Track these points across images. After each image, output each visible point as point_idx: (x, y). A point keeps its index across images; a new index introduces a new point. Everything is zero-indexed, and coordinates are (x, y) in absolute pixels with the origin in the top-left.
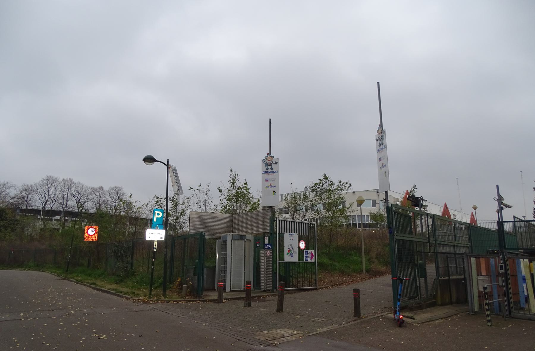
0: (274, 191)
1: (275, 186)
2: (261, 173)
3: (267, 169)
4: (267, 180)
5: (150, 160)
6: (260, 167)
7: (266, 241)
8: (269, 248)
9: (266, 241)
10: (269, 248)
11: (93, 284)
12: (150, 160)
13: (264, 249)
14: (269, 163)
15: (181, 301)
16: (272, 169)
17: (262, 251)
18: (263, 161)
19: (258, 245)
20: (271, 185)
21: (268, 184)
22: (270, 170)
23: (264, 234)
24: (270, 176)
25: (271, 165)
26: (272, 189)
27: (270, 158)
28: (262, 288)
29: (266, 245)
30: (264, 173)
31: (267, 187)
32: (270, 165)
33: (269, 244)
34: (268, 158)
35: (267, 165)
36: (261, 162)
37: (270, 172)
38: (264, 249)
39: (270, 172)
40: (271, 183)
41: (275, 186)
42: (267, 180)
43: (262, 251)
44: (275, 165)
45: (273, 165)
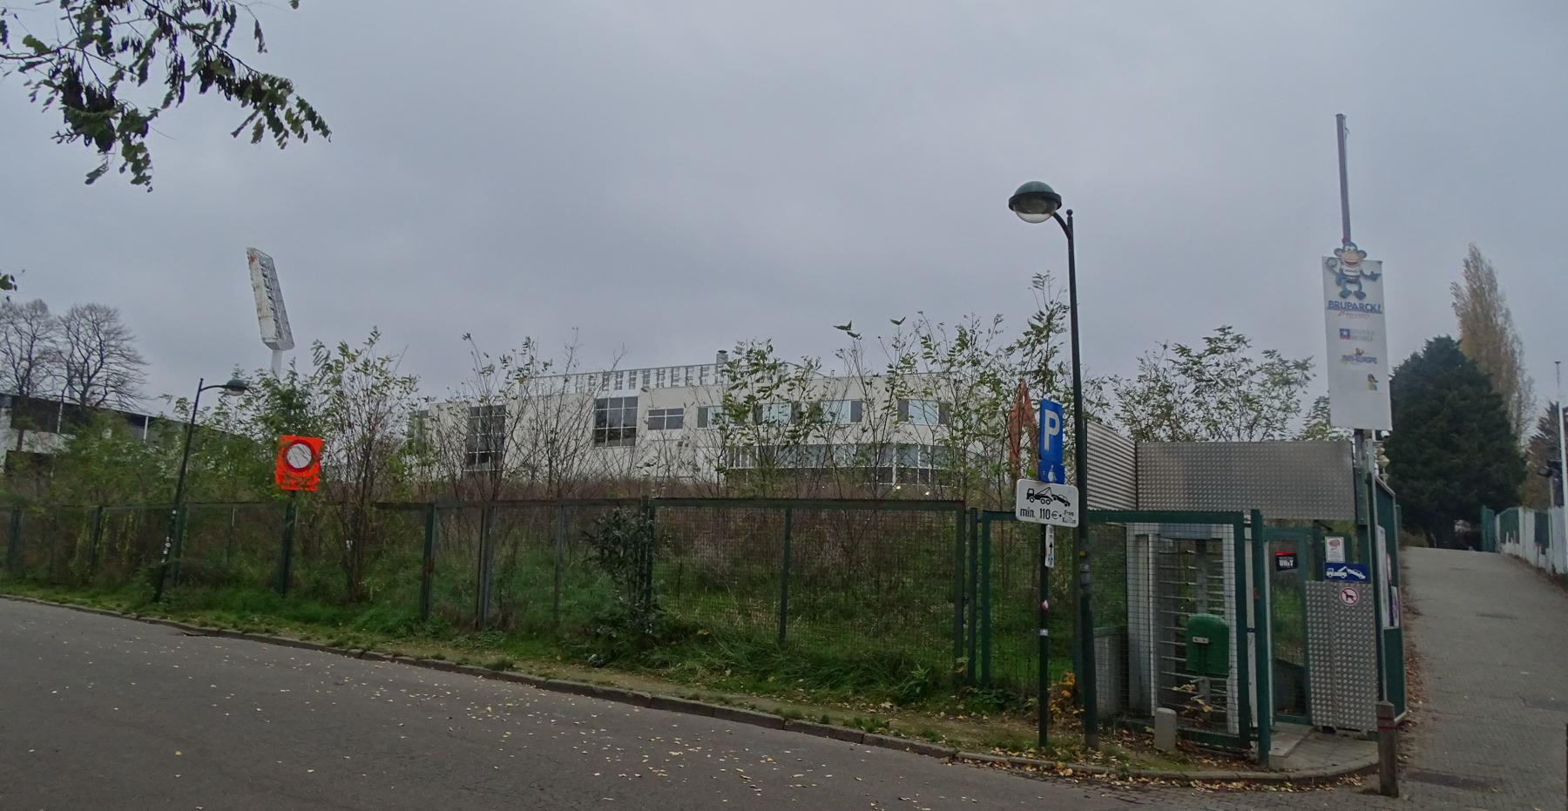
0: (1371, 377)
1: (1374, 360)
2: (1321, 305)
3: (1344, 295)
4: (1345, 334)
5: (1034, 200)
6: (1316, 288)
7: (1335, 550)
8: (1351, 578)
9: (1335, 550)
10: (1351, 578)
11: (510, 666)
12: (1034, 200)
13: (1320, 575)
14: (1350, 272)
15: (1229, 781)
16: (1360, 295)
17: (1310, 584)
18: (1329, 265)
19: (1283, 563)
20: (1359, 353)
21: (1349, 347)
22: (1352, 300)
23: (1323, 528)
24: (1356, 322)
25: (1355, 281)
26: (1365, 368)
27: (1354, 258)
28: (1321, 714)
29: (1337, 566)
30: (1332, 305)
31: (1346, 358)
32: (1351, 280)
33: (1349, 563)
34: (1346, 256)
35: (1342, 279)
36: (1319, 269)
37: (1355, 308)
38: (1320, 575)
39: (1355, 308)
40: (1362, 345)
41: (1374, 360)
42: (1345, 334)
43: (1310, 584)
44: (1370, 283)
45: (1362, 280)
